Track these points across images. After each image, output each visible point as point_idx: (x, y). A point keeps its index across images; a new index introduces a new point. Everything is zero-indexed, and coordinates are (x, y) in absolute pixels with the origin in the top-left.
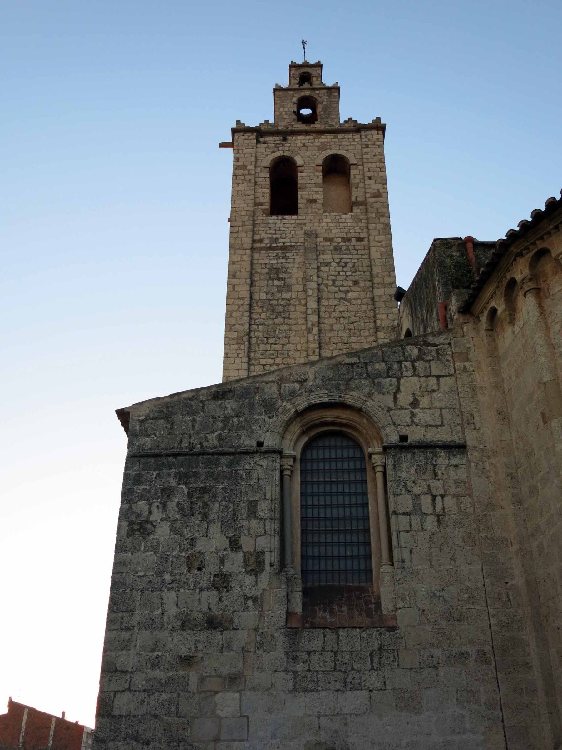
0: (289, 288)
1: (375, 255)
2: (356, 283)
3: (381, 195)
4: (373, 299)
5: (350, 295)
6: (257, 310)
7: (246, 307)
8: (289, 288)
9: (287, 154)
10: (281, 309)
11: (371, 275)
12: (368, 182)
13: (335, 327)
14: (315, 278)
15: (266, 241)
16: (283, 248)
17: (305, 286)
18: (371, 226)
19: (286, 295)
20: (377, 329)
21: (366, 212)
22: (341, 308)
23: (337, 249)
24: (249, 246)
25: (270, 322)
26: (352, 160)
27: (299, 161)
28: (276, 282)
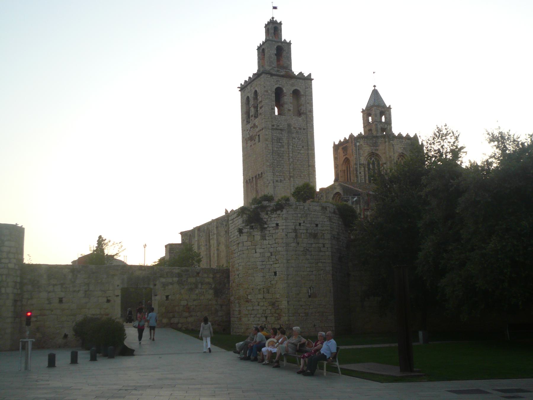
0: (283, 146)
2: (303, 147)
3: (311, 111)
4: (308, 154)
5: (302, 152)
6: (274, 154)
7: (271, 154)
8: (283, 146)
9: (280, 86)
10: (281, 155)
11: (308, 144)
13: (298, 163)
14: (291, 144)
15: (275, 126)
16: (281, 130)
17: (288, 146)
18: (308, 125)
19: (283, 149)
21: (306, 118)
22: (299, 156)
23: (297, 132)
24: (270, 128)
25: (278, 159)
26: (302, 93)
27: (285, 91)
28: (279, 144)
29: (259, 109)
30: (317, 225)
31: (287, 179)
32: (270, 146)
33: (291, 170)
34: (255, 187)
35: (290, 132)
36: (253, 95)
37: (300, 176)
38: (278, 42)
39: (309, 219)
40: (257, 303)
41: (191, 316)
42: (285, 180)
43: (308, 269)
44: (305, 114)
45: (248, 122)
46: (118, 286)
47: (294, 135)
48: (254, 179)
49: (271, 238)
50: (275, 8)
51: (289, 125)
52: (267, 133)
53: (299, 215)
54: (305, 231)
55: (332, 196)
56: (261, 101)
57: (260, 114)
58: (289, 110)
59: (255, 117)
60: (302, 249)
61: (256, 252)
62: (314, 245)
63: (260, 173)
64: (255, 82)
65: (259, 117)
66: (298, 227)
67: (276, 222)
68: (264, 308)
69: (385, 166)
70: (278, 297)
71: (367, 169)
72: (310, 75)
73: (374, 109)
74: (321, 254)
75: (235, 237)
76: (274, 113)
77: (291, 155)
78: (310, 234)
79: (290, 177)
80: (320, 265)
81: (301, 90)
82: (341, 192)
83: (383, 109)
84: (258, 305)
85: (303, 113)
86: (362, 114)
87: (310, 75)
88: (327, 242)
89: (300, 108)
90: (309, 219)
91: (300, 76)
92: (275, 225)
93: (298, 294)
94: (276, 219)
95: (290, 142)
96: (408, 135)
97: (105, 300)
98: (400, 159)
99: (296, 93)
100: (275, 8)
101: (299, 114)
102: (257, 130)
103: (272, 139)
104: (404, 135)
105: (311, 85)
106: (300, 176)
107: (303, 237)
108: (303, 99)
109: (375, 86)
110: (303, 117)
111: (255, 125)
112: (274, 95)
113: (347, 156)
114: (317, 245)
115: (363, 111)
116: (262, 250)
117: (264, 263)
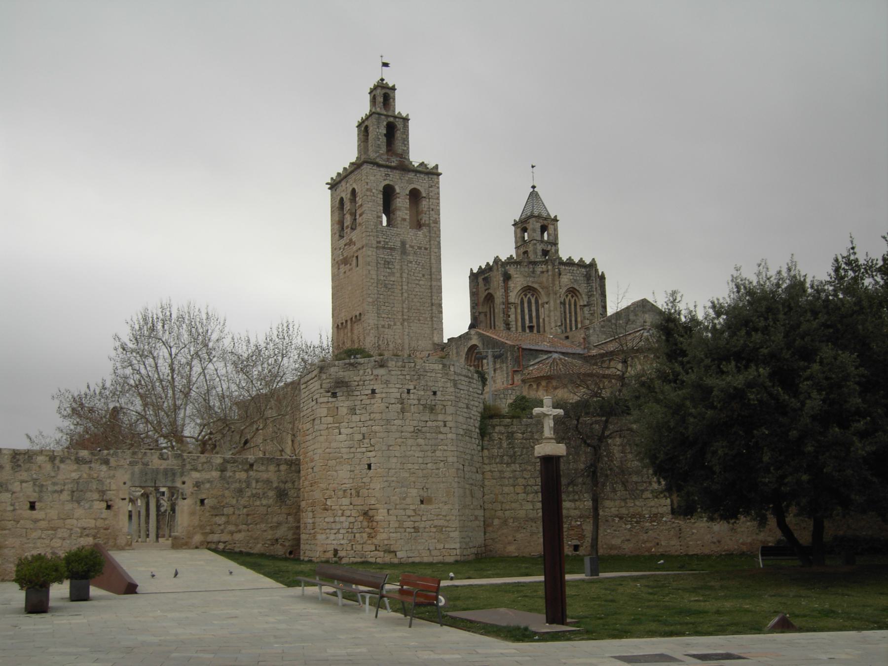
0: (393, 274)
1: (433, 261)
2: (424, 275)
3: (437, 222)
5: (421, 282)
8: (393, 274)
9: (391, 183)
10: (390, 286)
12: (431, 212)
14: (406, 271)
16: (391, 249)
18: (432, 242)
19: (393, 279)
20: (432, 305)
21: (430, 232)
24: (374, 246)
27: (398, 190)
29: (357, 217)
30: (435, 393)
31: (398, 324)
32: (373, 272)
33: (406, 310)
34: (349, 334)
35: (404, 252)
36: (349, 196)
37: (419, 320)
38: (387, 116)
39: (423, 382)
40: (340, 512)
41: (240, 531)
42: (395, 324)
43: (420, 460)
44: (429, 225)
45: (341, 237)
46: (125, 483)
47: (411, 258)
48: (349, 322)
49: (363, 411)
50: (385, 65)
51: (403, 244)
52: (370, 253)
53: (408, 377)
54: (416, 402)
55: (466, 350)
56: (361, 205)
57: (360, 224)
58: (404, 220)
59: (352, 229)
60: (412, 429)
61: (340, 434)
62: (430, 424)
63: (358, 314)
64: (353, 176)
65: (358, 228)
66: (405, 395)
67: (371, 387)
68: (352, 519)
69: (546, 306)
70: (373, 502)
71: (519, 311)
72: (436, 167)
73: (531, 221)
74: (441, 436)
75: (310, 410)
76: (381, 222)
77: (405, 287)
78: (425, 406)
79: (404, 320)
80: (438, 453)
81: (422, 190)
82: (480, 345)
83: (545, 222)
84: (343, 515)
85: (424, 225)
86: (513, 228)
87: (436, 167)
88: (449, 418)
89: (420, 217)
90: (423, 382)
91: (420, 169)
92: (370, 392)
93: (404, 499)
94: (372, 383)
95: (405, 267)
96: (581, 260)
97: (104, 505)
98: (570, 296)
99: (415, 196)
100: (385, 65)
101: (419, 225)
102: (355, 248)
103: (378, 263)
104: (576, 260)
105: (438, 183)
106: (419, 320)
107: (413, 411)
108: (424, 204)
109: (534, 187)
110: (425, 229)
111: (351, 240)
112: (381, 196)
113: (490, 291)
114: (435, 424)
115: (515, 224)
116: (350, 431)
117: (353, 450)
